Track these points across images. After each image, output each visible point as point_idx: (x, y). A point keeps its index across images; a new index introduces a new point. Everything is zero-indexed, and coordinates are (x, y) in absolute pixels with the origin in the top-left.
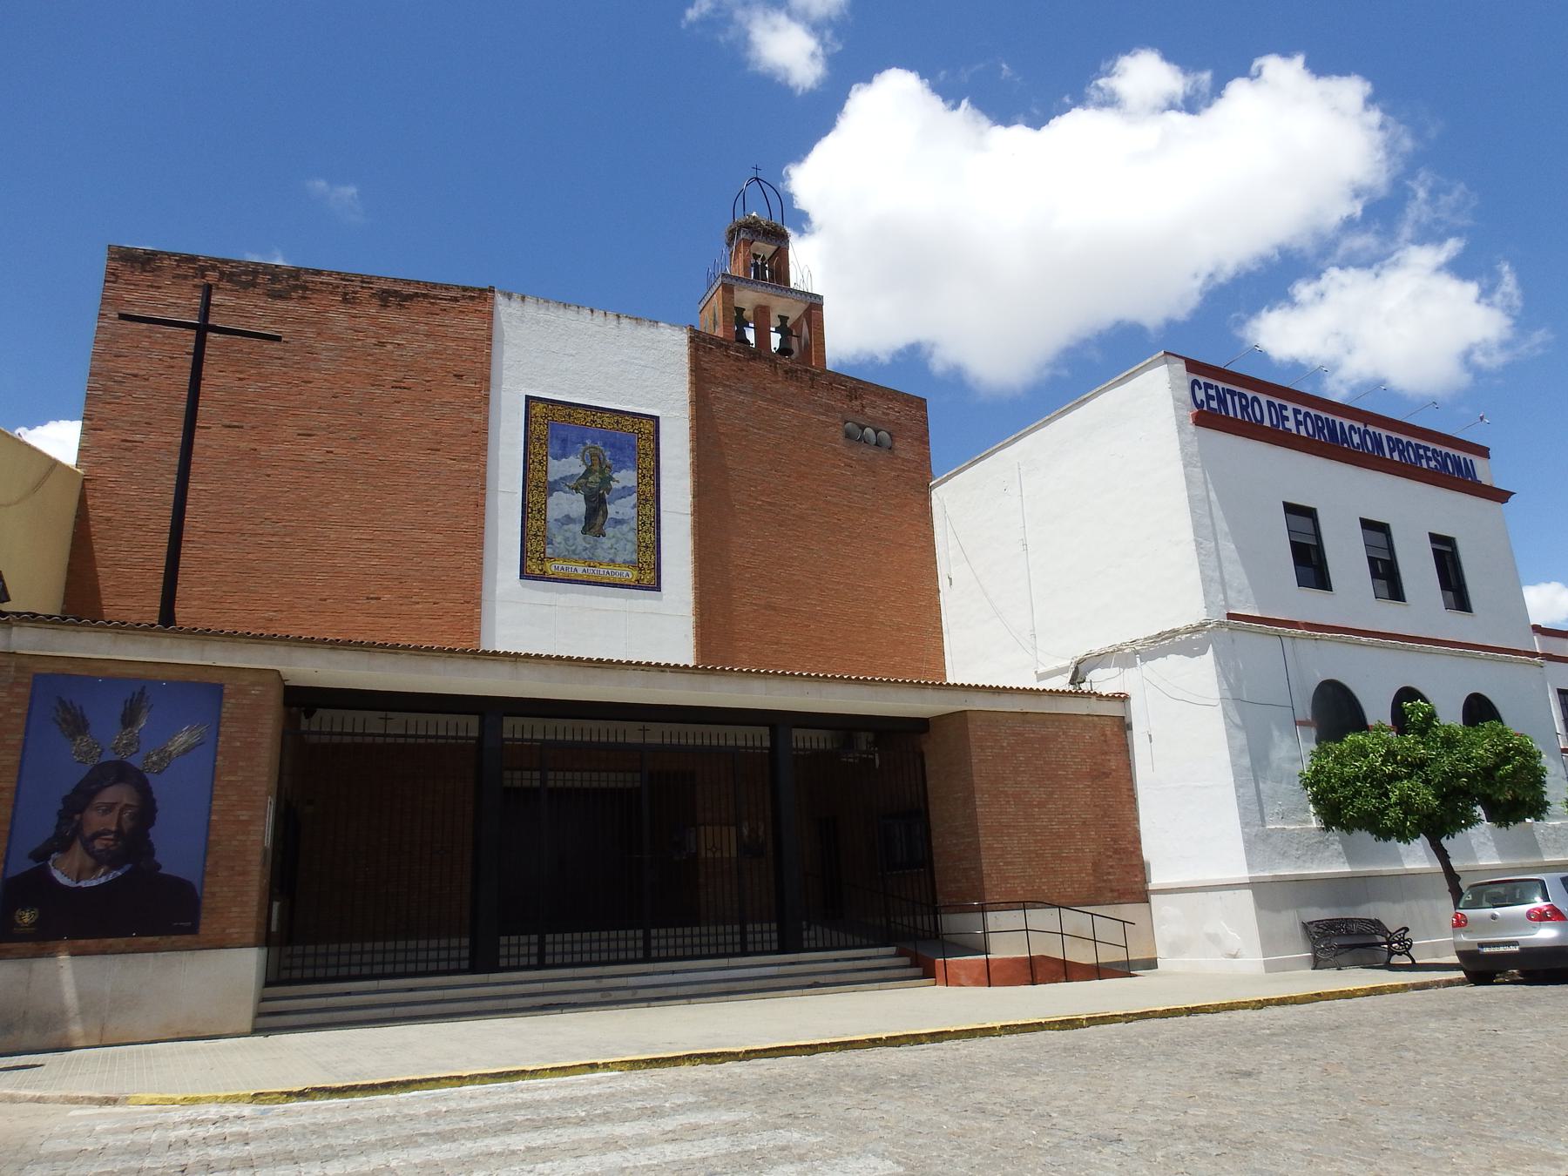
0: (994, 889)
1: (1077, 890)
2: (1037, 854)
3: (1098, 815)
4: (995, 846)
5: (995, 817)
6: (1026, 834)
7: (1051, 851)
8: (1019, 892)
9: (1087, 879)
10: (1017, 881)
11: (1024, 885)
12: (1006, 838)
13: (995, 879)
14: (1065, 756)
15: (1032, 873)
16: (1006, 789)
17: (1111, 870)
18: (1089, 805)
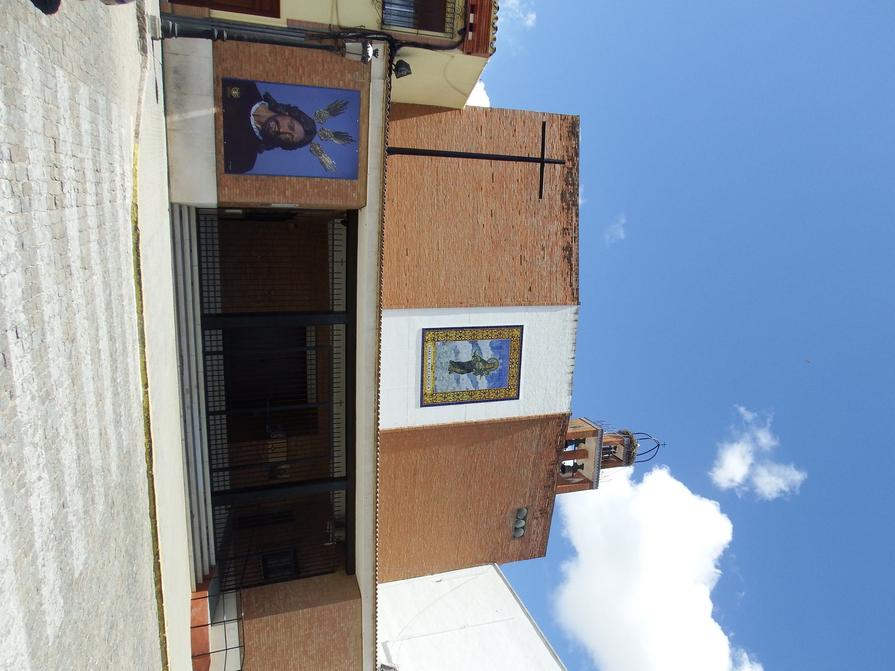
0: (251, 626)
4: (279, 624)
6: (287, 644)
10: (257, 641)
11: (255, 645)
12: (284, 630)
14: (336, 665)
15: (262, 650)
16: (314, 628)
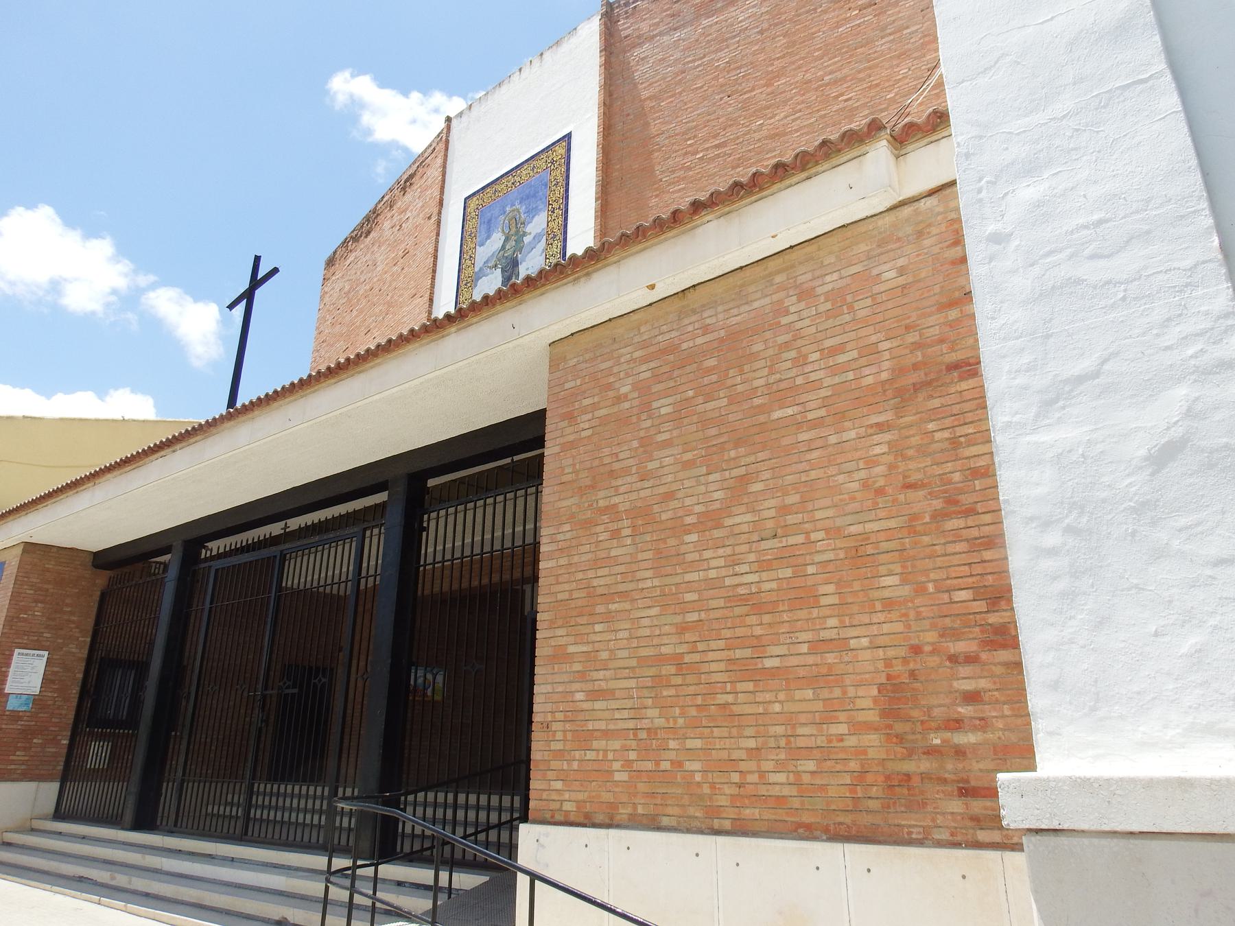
0: (555, 764)
1: (806, 778)
2: (679, 665)
3: (914, 517)
4: (571, 649)
5: (580, 576)
6: (655, 611)
7: (724, 655)
8: (618, 777)
9: (851, 741)
10: (616, 744)
11: (632, 755)
12: (598, 628)
13: (559, 736)
14: (800, 361)
15: (660, 722)
16: (616, 500)
17: (964, 710)
18: (880, 492)
